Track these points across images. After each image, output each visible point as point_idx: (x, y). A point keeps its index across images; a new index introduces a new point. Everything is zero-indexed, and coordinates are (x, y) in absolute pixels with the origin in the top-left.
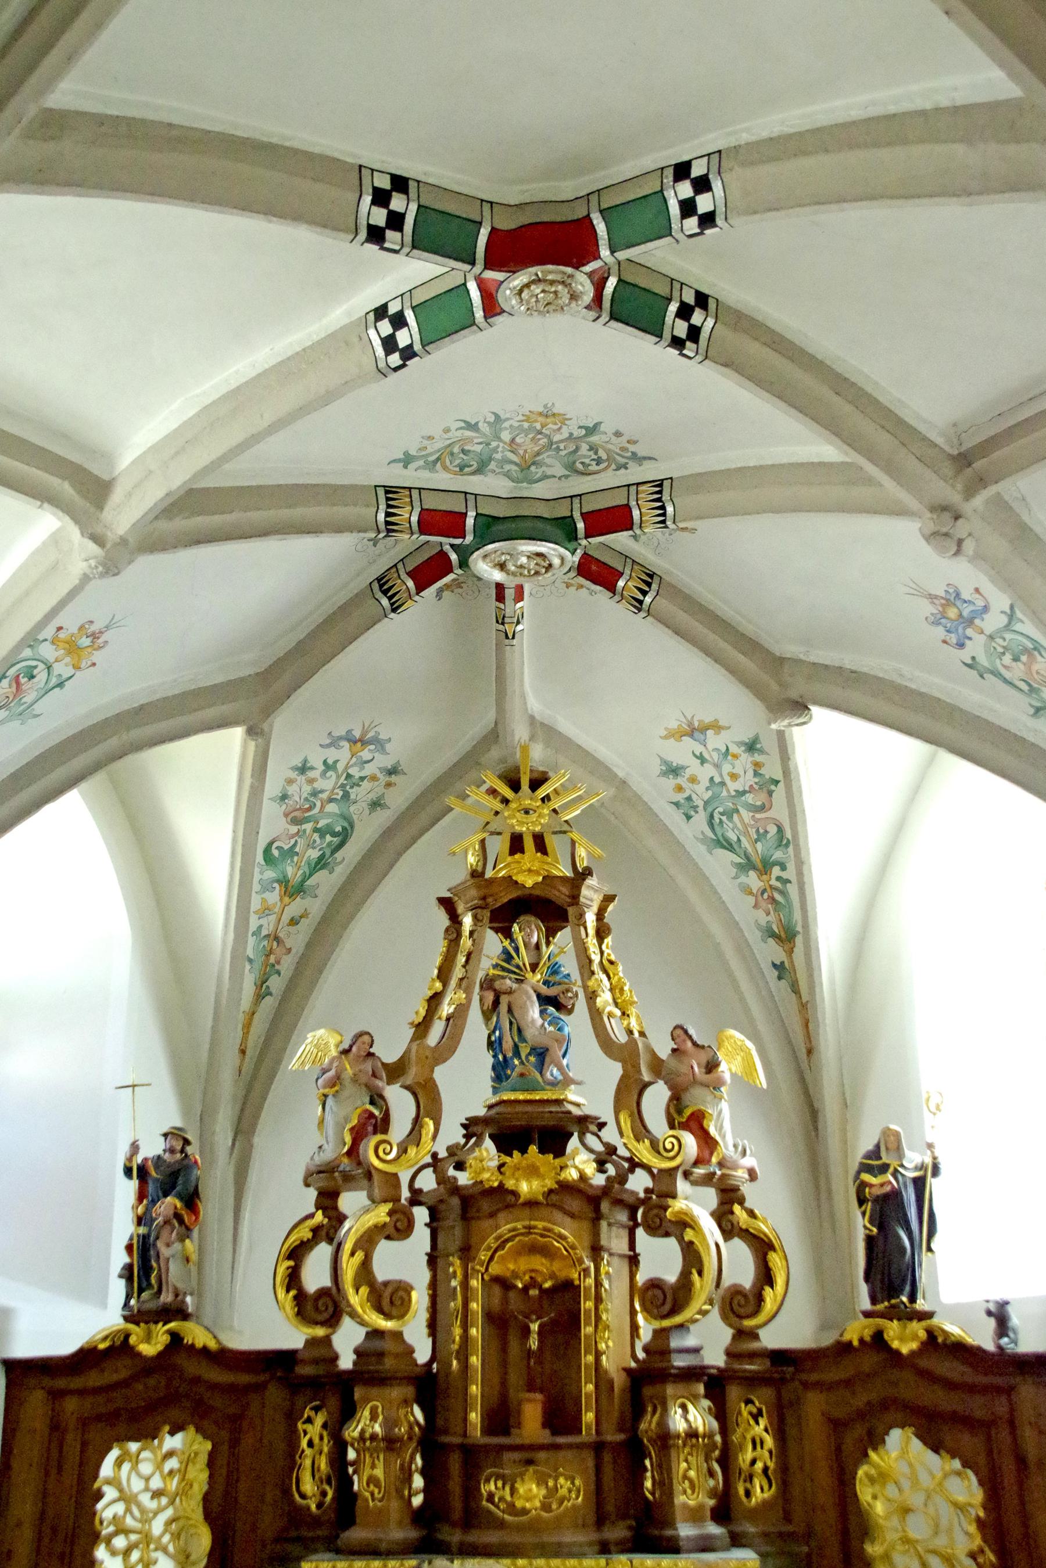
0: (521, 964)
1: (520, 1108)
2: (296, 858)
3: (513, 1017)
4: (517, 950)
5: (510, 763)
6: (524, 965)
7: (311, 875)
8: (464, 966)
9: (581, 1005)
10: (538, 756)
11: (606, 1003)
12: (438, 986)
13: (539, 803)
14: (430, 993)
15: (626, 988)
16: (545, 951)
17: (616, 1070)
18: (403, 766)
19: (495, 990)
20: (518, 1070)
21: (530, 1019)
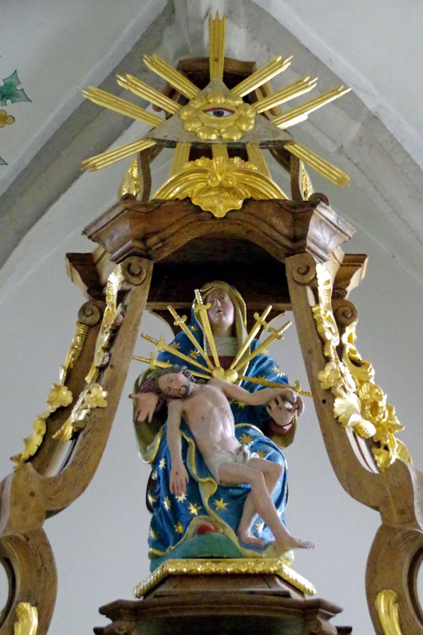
0: (205, 355)
1: (197, 588)
3: (191, 435)
4: (200, 335)
5: (193, 54)
6: (212, 359)
8: (106, 349)
9: (306, 423)
10: (238, 45)
11: (351, 410)
12: (66, 396)
13: (241, 102)
14: (51, 409)
15: (382, 404)
16: (247, 339)
17: (368, 522)
18: (24, 85)
19: (158, 392)
20: (195, 523)
21: (218, 438)
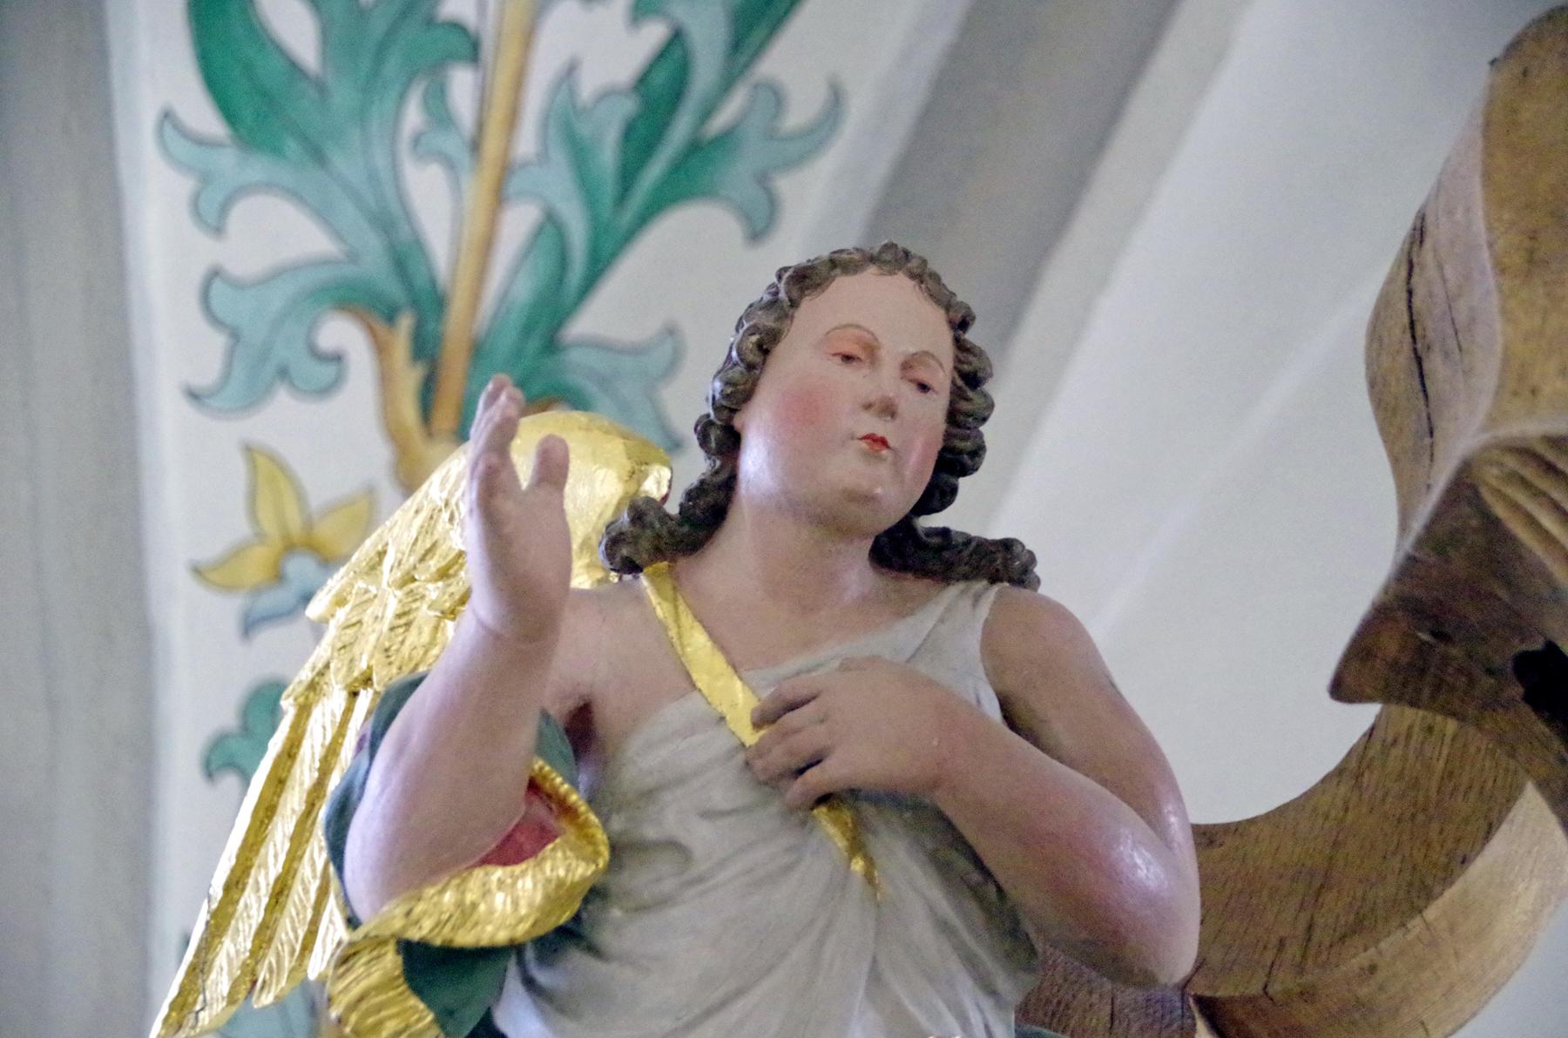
2: (462, 84)
7: (599, 266)
